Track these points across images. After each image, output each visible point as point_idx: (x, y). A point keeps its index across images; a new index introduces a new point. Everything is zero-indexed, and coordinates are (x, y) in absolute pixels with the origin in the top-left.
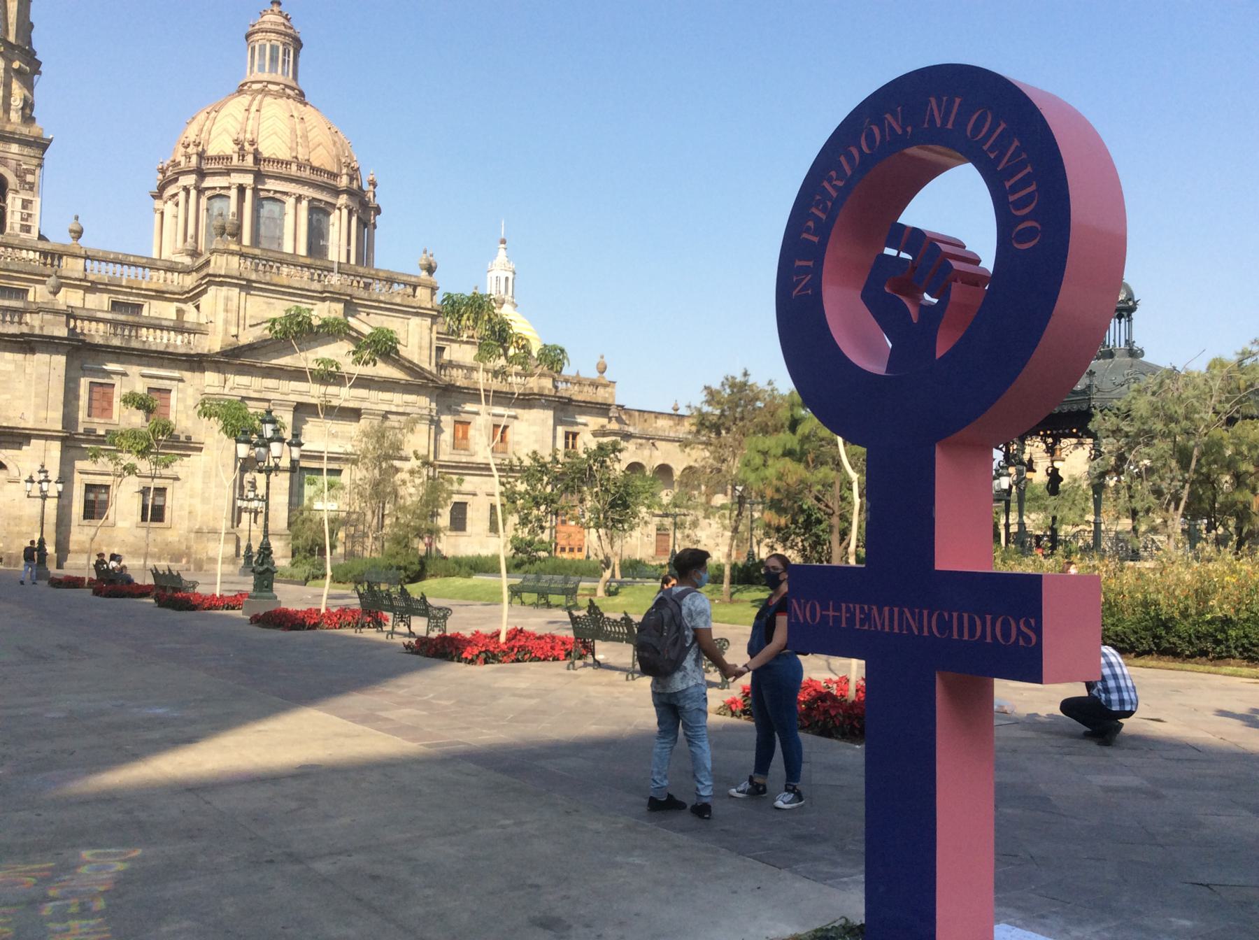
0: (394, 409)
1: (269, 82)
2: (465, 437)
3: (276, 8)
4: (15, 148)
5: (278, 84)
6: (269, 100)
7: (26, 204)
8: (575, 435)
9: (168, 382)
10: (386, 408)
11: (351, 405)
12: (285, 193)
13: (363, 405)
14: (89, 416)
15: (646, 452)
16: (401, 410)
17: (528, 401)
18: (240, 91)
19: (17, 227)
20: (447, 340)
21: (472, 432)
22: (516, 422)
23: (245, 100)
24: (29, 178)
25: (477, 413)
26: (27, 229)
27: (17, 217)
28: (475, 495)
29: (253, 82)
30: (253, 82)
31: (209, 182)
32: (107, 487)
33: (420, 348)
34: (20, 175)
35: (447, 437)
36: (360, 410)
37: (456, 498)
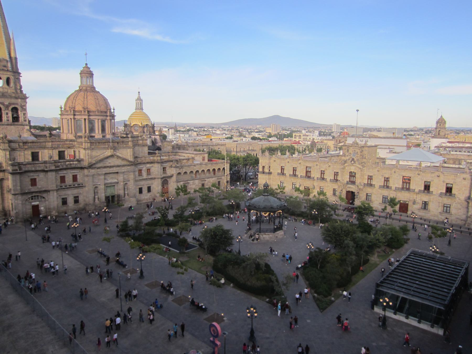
2: (141, 172)
4: (20, 100)
7: (24, 114)
8: (165, 168)
10: (123, 171)
13: (119, 171)
15: (181, 170)
19: (23, 120)
21: (142, 172)
24: (24, 107)
26: (25, 121)
27: (23, 118)
31: (76, 117)
32: (66, 198)
34: (22, 107)
35: (137, 173)
37: (140, 187)
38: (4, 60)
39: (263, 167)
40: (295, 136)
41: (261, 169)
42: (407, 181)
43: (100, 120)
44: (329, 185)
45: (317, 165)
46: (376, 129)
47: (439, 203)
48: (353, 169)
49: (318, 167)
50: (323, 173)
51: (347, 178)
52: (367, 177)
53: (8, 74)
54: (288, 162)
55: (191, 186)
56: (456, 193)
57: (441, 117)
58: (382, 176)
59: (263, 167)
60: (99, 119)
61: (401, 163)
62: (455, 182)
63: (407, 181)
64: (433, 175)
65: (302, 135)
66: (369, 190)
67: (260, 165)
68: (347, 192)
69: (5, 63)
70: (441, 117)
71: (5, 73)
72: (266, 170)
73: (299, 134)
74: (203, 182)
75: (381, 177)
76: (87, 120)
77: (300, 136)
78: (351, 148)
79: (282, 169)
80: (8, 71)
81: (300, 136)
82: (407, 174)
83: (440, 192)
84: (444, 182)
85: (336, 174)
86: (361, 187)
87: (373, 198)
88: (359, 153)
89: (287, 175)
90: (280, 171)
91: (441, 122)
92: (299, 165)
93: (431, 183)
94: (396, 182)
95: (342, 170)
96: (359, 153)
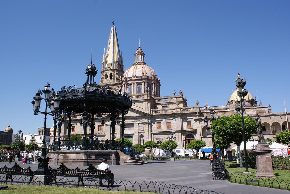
0: (140, 122)
1: (139, 62)
3: (140, 49)
5: (140, 62)
6: (138, 65)
9: (160, 121)
10: (139, 122)
11: (131, 123)
12: (131, 83)
14: (98, 131)
16: (142, 122)
17: (173, 116)
18: (134, 65)
20: (168, 104)
22: (172, 121)
23: (133, 67)
25: (162, 120)
28: (163, 139)
29: (136, 63)
30: (136, 63)
33: (145, 108)
36: (133, 123)
38: (110, 64)
43: (135, 84)
53: (111, 71)
60: (134, 83)
69: (110, 66)
71: (109, 71)
76: (125, 85)
80: (110, 70)
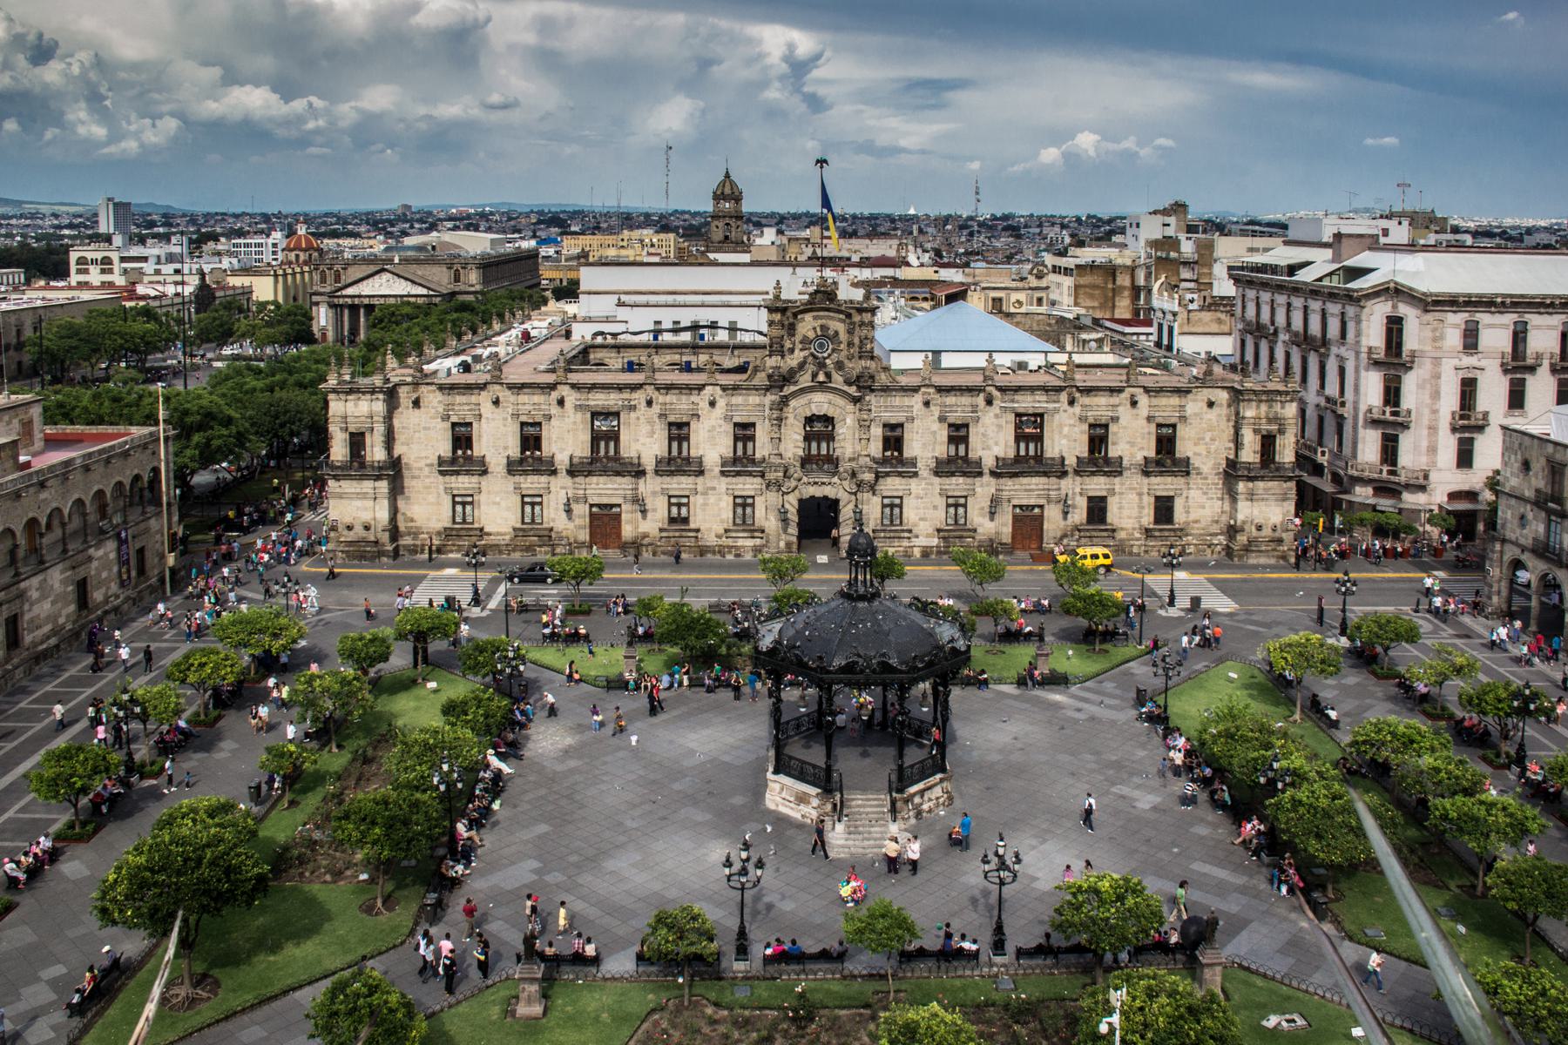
39: (357, 441)
40: (81, 261)
41: (339, 450)
42: (1030, 428)
44: (714, 483)
45: (649, 403)
46: (484, 216)
47: (1140, 494)
48: (820, 403)
49: (656, 409)
50: (679, 431)
51: (793, 444)
52: (877, 431)
54: (496, 402)
55: (36, 610)
56: (1190, 454)
57: (727, 176)
58: (942, 419)
59: (357, 441)
61: (947, 361)
62: (1183, 418)
63: (1030, 428)
64: (1115, 400)
65: (115, 256)
66: (892, 485)
67: (334, 429)
68: (837, 501)
70: (727, 176)
72: (376, 452)
73: (99, 256)
74: (81, 573)
75: (936, 426)
77: (107, 261)
78: (808, 317)
79: (462, 438)
81: (107, 261)
82: (1026, 403)
83: (1139, 457)
84: (1149, 419)
85: (744, 432)
86: (868, 477)
87: (911, 513)
88: (843, 336)
89: (497, 463)
90: (445, 448)
91: (728, 192)
92: (555, 410)
93: (1113, 428)
94: (993, 438)
95: (776, 414)
96: (843, 336)
